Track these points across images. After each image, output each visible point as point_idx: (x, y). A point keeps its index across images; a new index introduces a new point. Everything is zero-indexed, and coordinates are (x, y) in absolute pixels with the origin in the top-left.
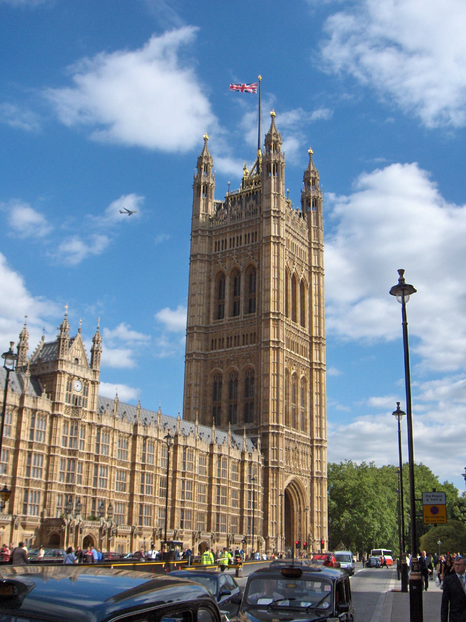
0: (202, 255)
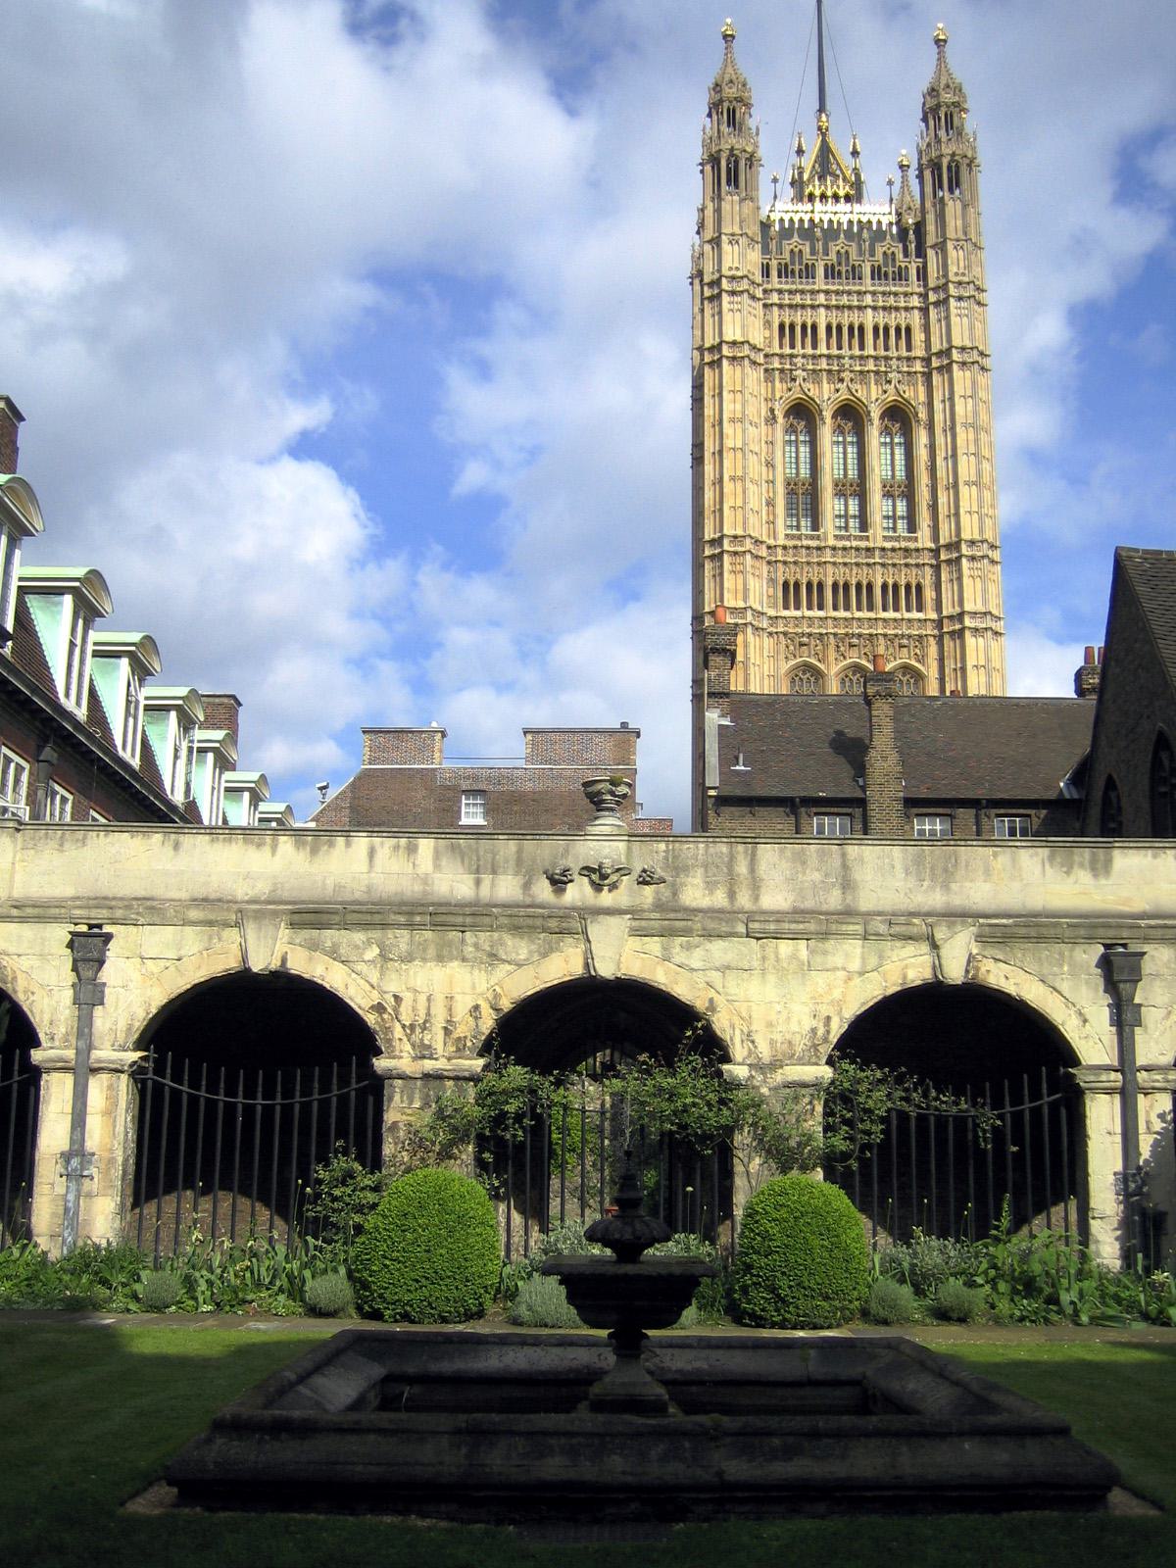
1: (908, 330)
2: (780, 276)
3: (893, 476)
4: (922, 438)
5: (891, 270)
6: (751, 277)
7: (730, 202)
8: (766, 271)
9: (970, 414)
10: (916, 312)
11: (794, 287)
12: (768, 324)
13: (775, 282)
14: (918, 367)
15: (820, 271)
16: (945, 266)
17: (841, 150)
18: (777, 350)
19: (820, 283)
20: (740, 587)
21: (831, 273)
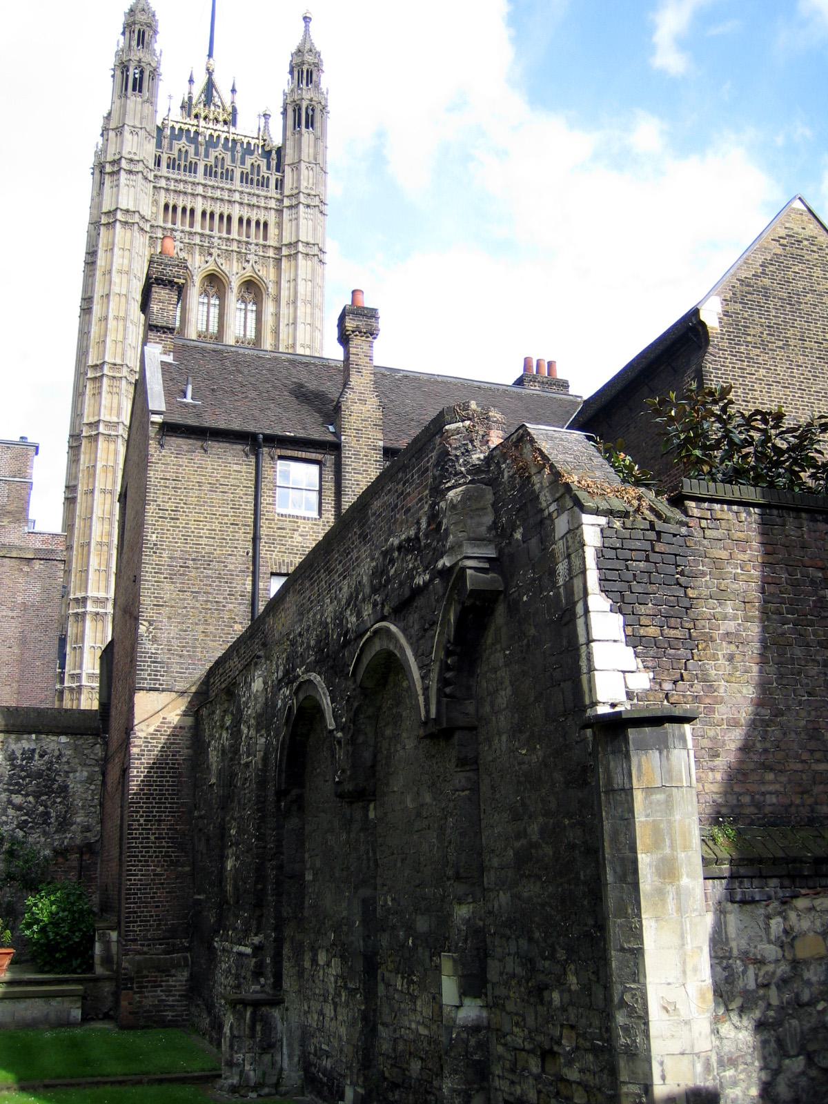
1: (266, 225)
2: (168, 167)
3: (245, 335)
4: (269, 307)
5: (255, 178)
6: (145, 162)
7: (134, 101)
8: (158, 162)
9: (309, 294)
10: (273, 212)
11: (179, 177)
12: (155, 202)
13: (164, 170)
14: (271, 253)
15: (201, 169)
16: (299, 180)
17: (223, 86)
18: (161, 224)
19: (200, 177)
20: (115, 405)
21: (209, 172)
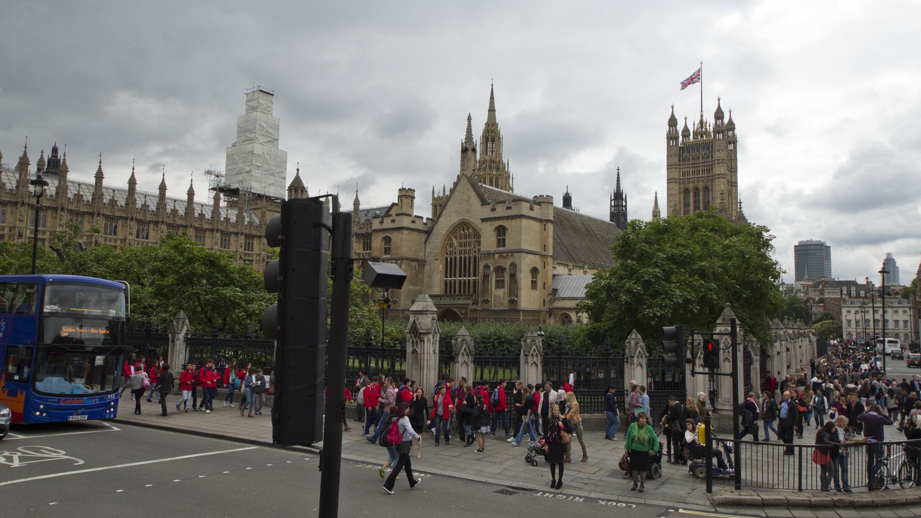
0: (676, 179)
8: (680, 160)
12: (680, 172)
18: (682, 177)
